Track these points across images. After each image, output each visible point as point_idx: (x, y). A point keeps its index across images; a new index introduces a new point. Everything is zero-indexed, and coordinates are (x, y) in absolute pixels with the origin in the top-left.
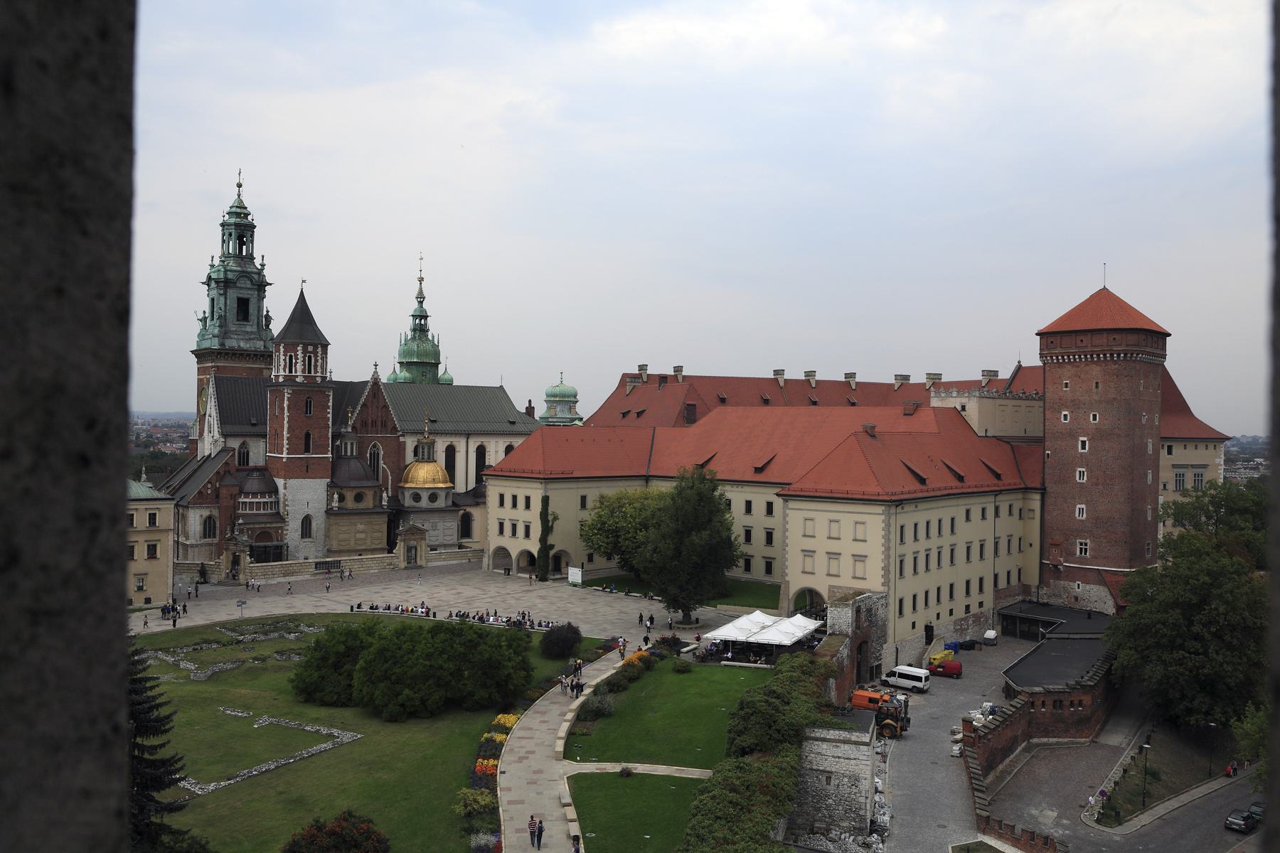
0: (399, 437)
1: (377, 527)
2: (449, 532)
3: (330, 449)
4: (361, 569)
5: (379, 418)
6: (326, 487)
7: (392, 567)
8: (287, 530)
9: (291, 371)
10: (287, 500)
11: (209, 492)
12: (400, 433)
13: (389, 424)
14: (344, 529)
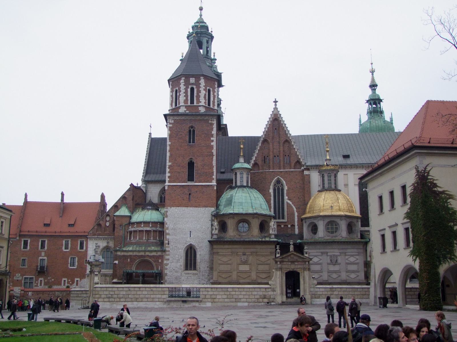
0: (303, 171)
1: (263, 259)
2: (354, 267)
3: (214, 177)
4: (226, 300)
5: (282, 155)
6: (210, 216)
7: (266, 300)
8: (168, 260)
9: (176, 105)
10: (168, 228)
11: (108, 224)
12: (305, 167)
13: (292, 158)
14: (225, 259)
